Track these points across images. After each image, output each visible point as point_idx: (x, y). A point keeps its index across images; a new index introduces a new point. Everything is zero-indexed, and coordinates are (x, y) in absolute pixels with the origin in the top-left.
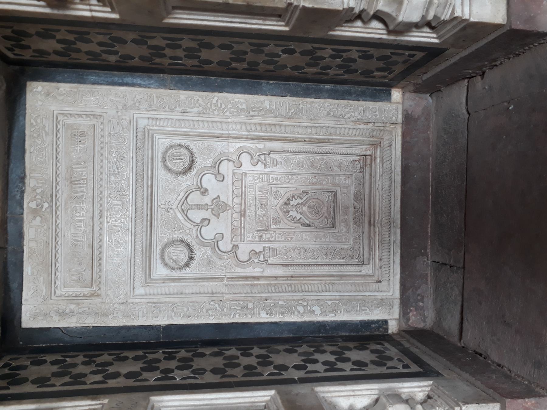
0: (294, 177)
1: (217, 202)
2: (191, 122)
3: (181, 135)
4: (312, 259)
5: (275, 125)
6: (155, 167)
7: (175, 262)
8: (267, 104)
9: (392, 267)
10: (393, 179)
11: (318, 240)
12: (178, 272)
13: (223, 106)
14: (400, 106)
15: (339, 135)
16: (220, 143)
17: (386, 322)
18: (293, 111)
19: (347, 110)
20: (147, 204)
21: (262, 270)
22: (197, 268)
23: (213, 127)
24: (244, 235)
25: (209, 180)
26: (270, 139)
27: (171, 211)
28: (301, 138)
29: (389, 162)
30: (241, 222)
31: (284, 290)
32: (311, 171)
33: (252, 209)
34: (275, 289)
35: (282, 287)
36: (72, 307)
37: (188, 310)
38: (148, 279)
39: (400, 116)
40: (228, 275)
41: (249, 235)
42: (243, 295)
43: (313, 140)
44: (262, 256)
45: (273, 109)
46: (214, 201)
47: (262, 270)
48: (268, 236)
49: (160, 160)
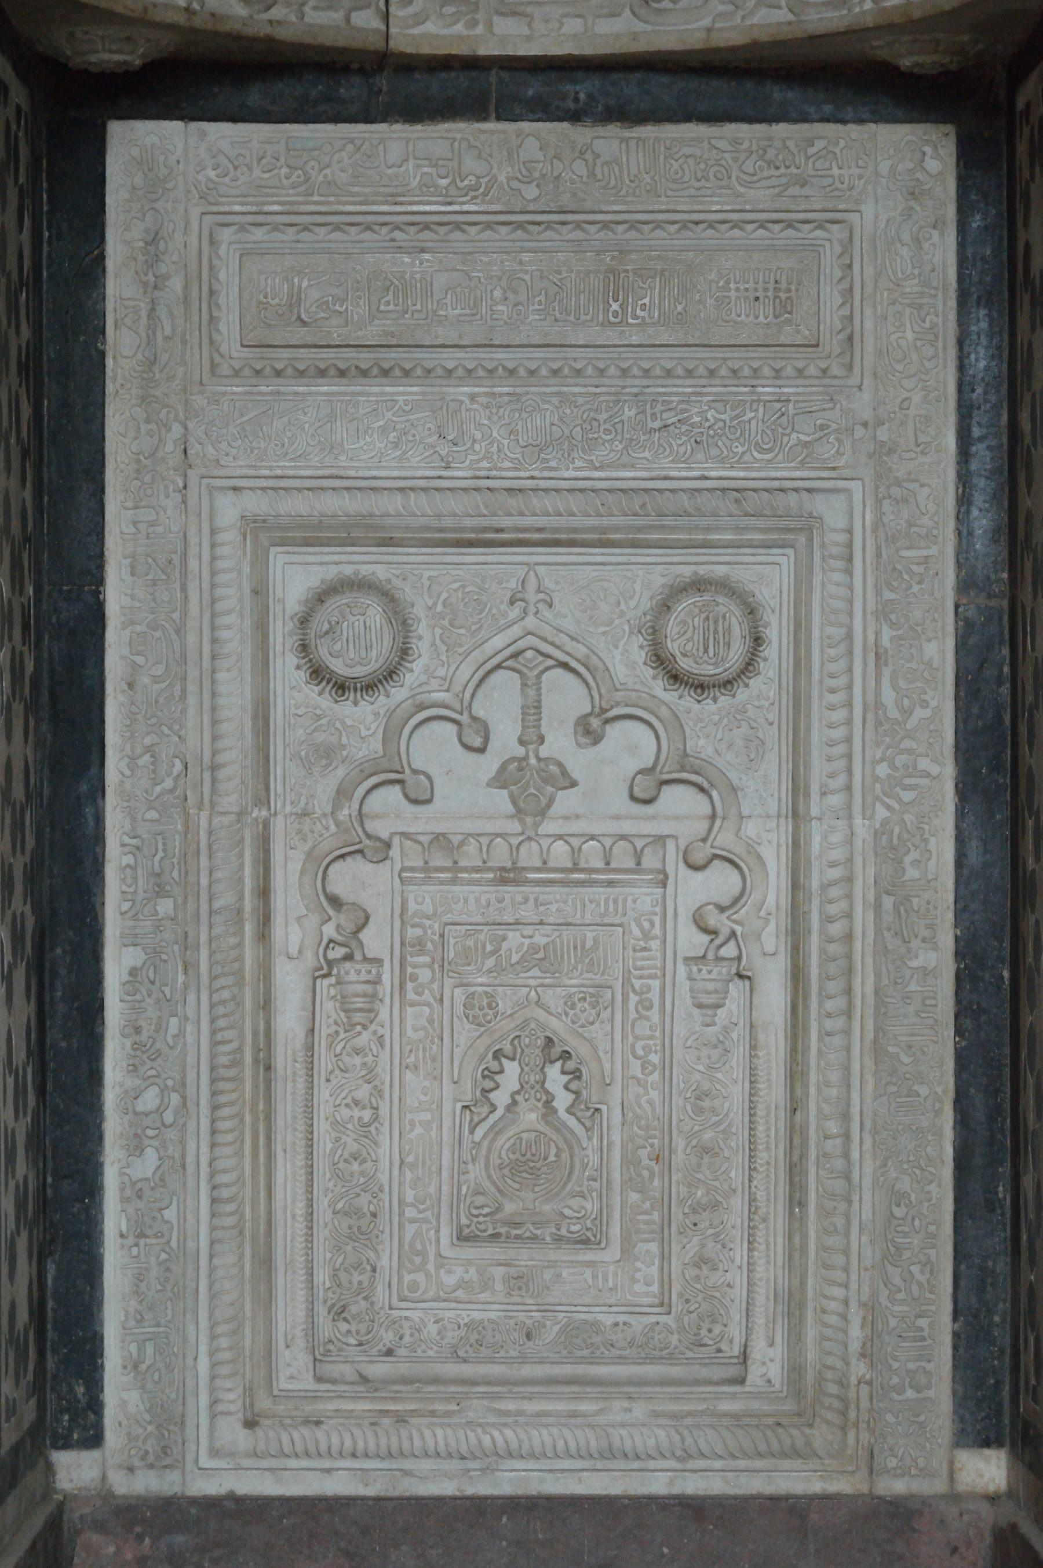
0: (656, 1076)
2: (842, 681)
4: (334, 1151)
5: (849, 991)
6: (677, 555)
9: (305, 1463)
10: (651, 1464)
13: (907, 796)
14: (938, 1486)
17: (94, 1440)
19: (915, 1269)
21: (294, 951)
24: (425, 881)
25: (633, 749)
26: (797, 975)
30: (477, 870)
31: (219, 1037)
32: (680, 1143)
33: (528, 913)
34: (223, 1002)
35: (231, 1027)
36: (176, 284)
37: (156, 680)
38: (266, 534)
39: (899, 1487)
40: (278, 826)
41: (423, 898)
42: (204, 881)
47: (294, 951)
48: (425, 975)
49: (702, 570)
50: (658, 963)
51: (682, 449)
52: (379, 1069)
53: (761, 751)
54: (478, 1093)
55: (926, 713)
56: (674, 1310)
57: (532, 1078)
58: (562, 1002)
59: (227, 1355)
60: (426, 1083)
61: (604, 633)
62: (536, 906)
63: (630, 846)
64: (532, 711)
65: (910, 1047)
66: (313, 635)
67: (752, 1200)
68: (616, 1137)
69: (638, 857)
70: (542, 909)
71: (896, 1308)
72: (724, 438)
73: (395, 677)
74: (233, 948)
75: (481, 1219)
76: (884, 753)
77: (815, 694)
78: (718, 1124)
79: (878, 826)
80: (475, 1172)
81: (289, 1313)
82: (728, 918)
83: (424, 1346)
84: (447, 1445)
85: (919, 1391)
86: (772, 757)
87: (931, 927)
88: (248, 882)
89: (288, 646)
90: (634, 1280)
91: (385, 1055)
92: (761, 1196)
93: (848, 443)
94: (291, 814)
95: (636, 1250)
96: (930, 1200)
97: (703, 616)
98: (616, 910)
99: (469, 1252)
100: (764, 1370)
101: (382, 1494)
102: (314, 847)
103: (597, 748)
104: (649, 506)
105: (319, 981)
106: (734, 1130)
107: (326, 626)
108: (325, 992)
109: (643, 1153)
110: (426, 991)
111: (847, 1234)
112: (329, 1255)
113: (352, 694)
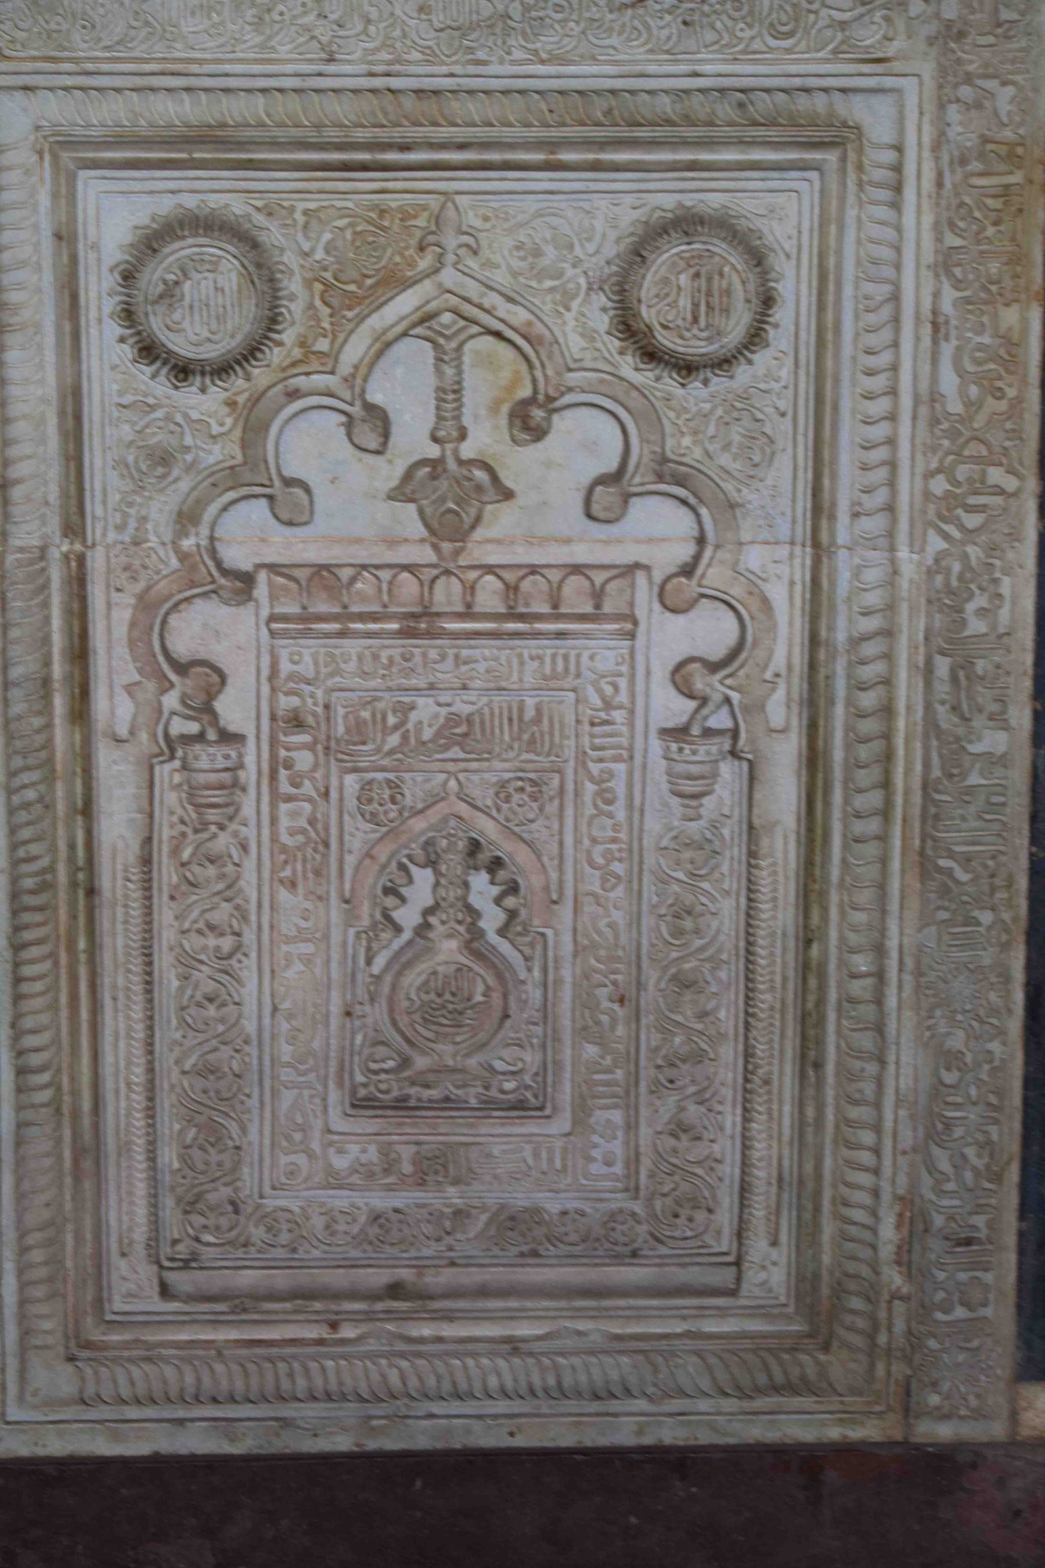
0: (620, 891)
1: (479, 488)
3: (821, 308)
4: (181, 989)
5: (886, 784)
6: (655, 181)
7: (169, 294)
8: (992, 741)
9: (150, 1412)
10: (614, 1406)
11: (285, 1026)
12: (110, 305)
13: (972, 521)
14: (997, 1430)
15: (844, 1121)
16: (785, 503)
18: (963, 876)
19: (970, 1152)
20: (462, 147)
22: (128, 399)
23: (865, 468)
24: (306, 634)
26: (814, 759)
27: (424, 263)
28: (825, 919)
29: (705, 1384)
30: (374, 617)
31: (21, 853)
32: (652, 976)
33: (446, 673)
34: (26, 806)
35: (37, 839)
39: (945, 1432)
40: (97, 561)
41: (302, 656)
43: (813, 983)
44: (194, 728)
45: (964, 775)
46: (480, 475)
47: (123, 731)
48: (304, 760)
49: (688, 200)
50: (624, 741)
51: (665, 33)
52: (242, 883)
53: (768, 450)
54: (378, 916)
55: (1002, 406)
56: (642, 1193)
57: (452, 894)
58: (492, 791)
59: (42, 1272)
60: (308, 905)
61: (552, 290)
62: (457, 666)
63: (586, 583)
64: (451, 397)
65: (968, 860)
66: (141, 299)
67: (748, 1054)
68: (566, 973)
69: (598, 596)
70: (464, 668)
71: (946, 1202)
72: (724, 17)
73: (259, 355)
74: (38, 731)
75: (383, 1076)
76: (941, 461)
77: (846, 375)
78: (702, 949)
79: (930, 562)
80: (377, 1014)
81: (127, 1210)
82: (721, 682)
83: (307, 1245)
84: (341, 1384)
85: (971, 1309)
86: (784, 463)
87: (1000, 700)
88: (58, 641)
89: (107, 309)
90: (590, 1159)
91: (250, 864)
92: (760, 1049)
93: (900, 25)
94: (115, 543)
95: (592, 1120)
96: (991, 1061)
97: (692, 271)
98: (567, 670)
99: (367, 1125)
100: (763, 1276)
101: (255, 1451)
102: (149, 588)
103: (540, 445)
104: (616, 112)
105: (157, 769)
106: (724, 957)
107: (161, 287)
108: (166, 780)
109: (603, 993)
110: (307, 782)
111: (878, 1105)
112: (177, 1127)
113: (198, 379)
